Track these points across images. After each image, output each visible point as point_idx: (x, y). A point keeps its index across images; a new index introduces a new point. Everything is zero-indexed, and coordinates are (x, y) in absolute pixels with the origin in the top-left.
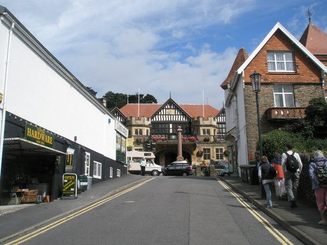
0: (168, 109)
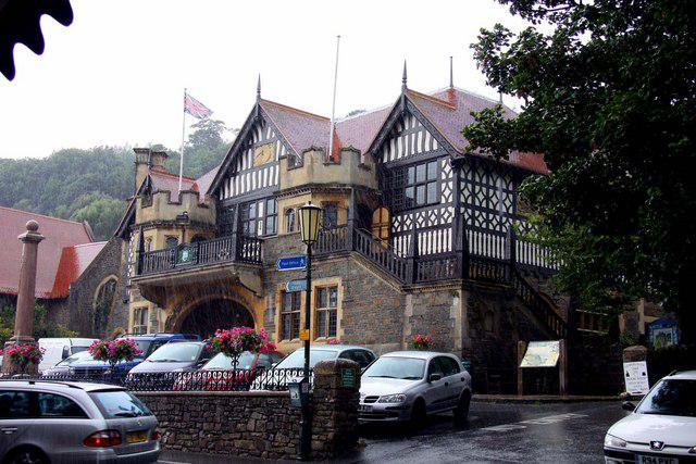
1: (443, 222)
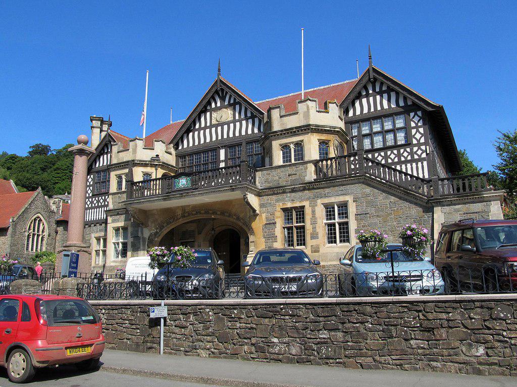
0: (217, 109)
1: (403, 159)
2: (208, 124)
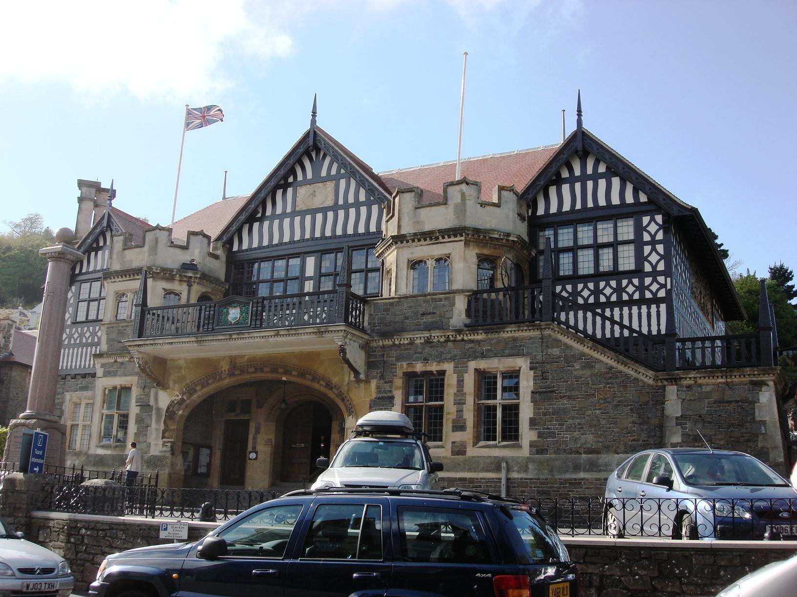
0: (306, 182)
2: (289, 210)
